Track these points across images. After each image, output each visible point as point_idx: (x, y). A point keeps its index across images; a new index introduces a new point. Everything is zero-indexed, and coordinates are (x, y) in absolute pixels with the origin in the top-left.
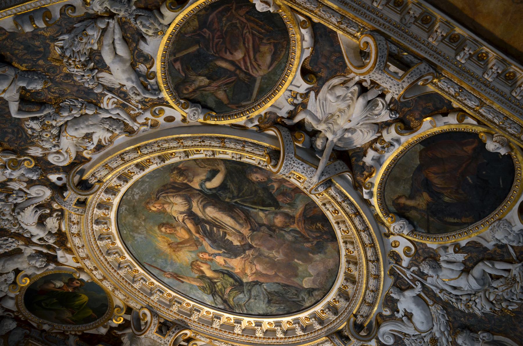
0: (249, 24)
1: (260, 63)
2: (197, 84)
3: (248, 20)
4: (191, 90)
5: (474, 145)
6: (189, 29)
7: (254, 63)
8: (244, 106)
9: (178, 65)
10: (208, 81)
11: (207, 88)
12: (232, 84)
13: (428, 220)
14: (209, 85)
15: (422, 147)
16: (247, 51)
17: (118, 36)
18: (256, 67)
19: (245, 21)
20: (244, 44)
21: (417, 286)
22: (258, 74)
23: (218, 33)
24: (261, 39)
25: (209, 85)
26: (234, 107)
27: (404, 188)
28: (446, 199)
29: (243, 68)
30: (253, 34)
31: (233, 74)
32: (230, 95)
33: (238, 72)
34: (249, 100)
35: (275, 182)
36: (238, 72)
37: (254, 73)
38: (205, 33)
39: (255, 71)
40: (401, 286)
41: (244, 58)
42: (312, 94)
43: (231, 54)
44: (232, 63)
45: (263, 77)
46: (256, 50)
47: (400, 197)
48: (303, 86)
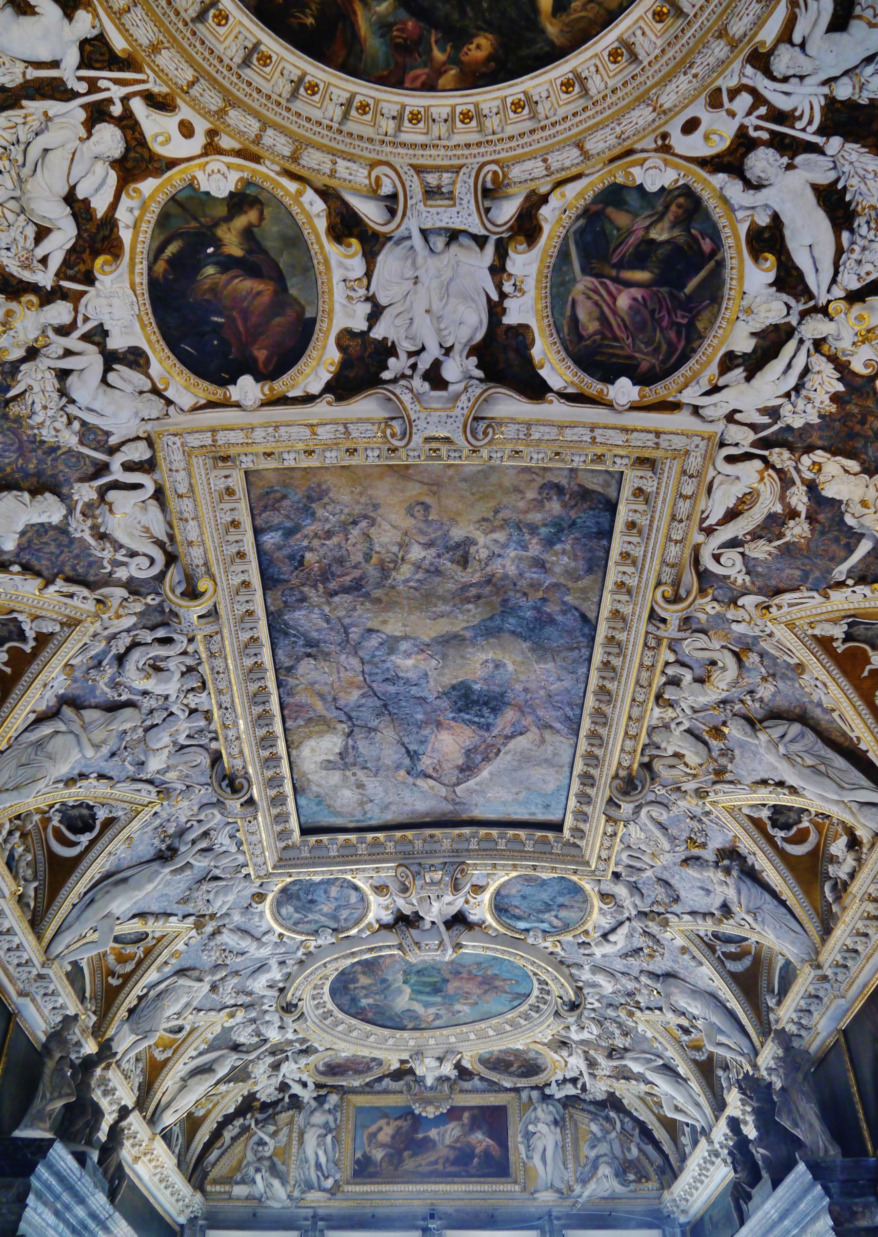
0: (628, 351)
1: (589, 303)
2: (666, 223)
3: (632, 358)
4: (673, 208)
5: (261, 365)
6: (706, 315)
7: (596, 297)
8: (578, 218)
9: (707, 245)
10: (653, 235)
11: (647, 222)
12: (613, 246)
13: (195, 218)
14: (647, 229)
15: (308, 315)
16: (615, 312)
17: (811, 280)
18: (592, 294)
19: (637, 355)
20: (623, 320)
21: (80, 79)
22: (583, 283)
23: (665, 324)
24: (604, 337)
25: (647, 229)
26: (595, 208)
27: (270, 234)
28: (210, 270)
29: (608, 282)
30: (616, 338)
31: (621, 265)
32: (608, 226)
33: (614, 273)
34: (575, 233)
35: (444, 64)
36: (614, 273)
37: (588, 281)
38: (683, 317)
39: (590, 285)
40: (95, 52)
41: (615, 299)
42: (495, 297)
43: (635, 299)
44: (628, 284)
45: (574, 281)
46: (603, 319)
47: (261, 217)
48: (517, 313)
